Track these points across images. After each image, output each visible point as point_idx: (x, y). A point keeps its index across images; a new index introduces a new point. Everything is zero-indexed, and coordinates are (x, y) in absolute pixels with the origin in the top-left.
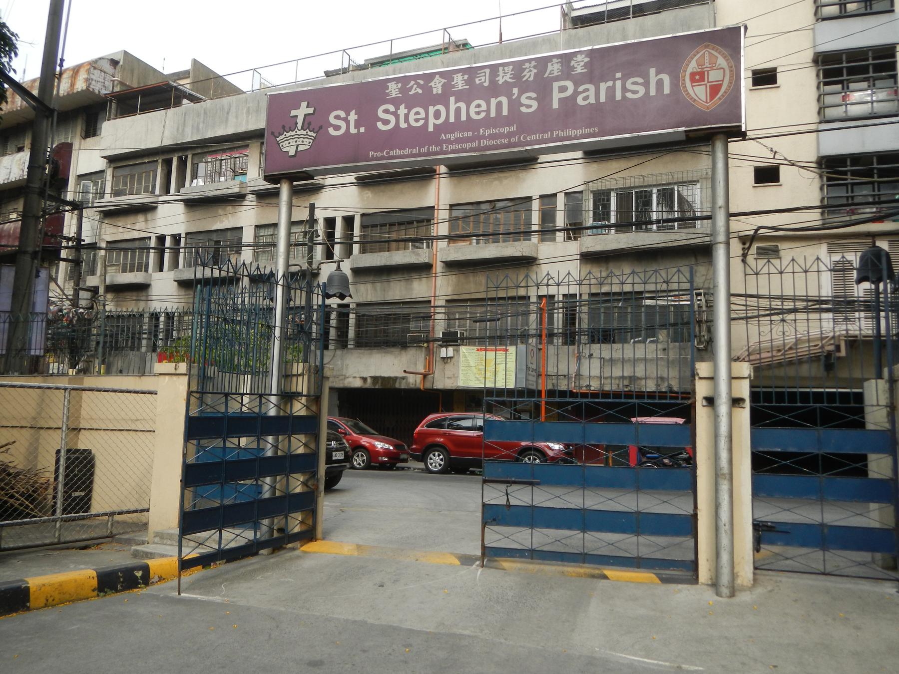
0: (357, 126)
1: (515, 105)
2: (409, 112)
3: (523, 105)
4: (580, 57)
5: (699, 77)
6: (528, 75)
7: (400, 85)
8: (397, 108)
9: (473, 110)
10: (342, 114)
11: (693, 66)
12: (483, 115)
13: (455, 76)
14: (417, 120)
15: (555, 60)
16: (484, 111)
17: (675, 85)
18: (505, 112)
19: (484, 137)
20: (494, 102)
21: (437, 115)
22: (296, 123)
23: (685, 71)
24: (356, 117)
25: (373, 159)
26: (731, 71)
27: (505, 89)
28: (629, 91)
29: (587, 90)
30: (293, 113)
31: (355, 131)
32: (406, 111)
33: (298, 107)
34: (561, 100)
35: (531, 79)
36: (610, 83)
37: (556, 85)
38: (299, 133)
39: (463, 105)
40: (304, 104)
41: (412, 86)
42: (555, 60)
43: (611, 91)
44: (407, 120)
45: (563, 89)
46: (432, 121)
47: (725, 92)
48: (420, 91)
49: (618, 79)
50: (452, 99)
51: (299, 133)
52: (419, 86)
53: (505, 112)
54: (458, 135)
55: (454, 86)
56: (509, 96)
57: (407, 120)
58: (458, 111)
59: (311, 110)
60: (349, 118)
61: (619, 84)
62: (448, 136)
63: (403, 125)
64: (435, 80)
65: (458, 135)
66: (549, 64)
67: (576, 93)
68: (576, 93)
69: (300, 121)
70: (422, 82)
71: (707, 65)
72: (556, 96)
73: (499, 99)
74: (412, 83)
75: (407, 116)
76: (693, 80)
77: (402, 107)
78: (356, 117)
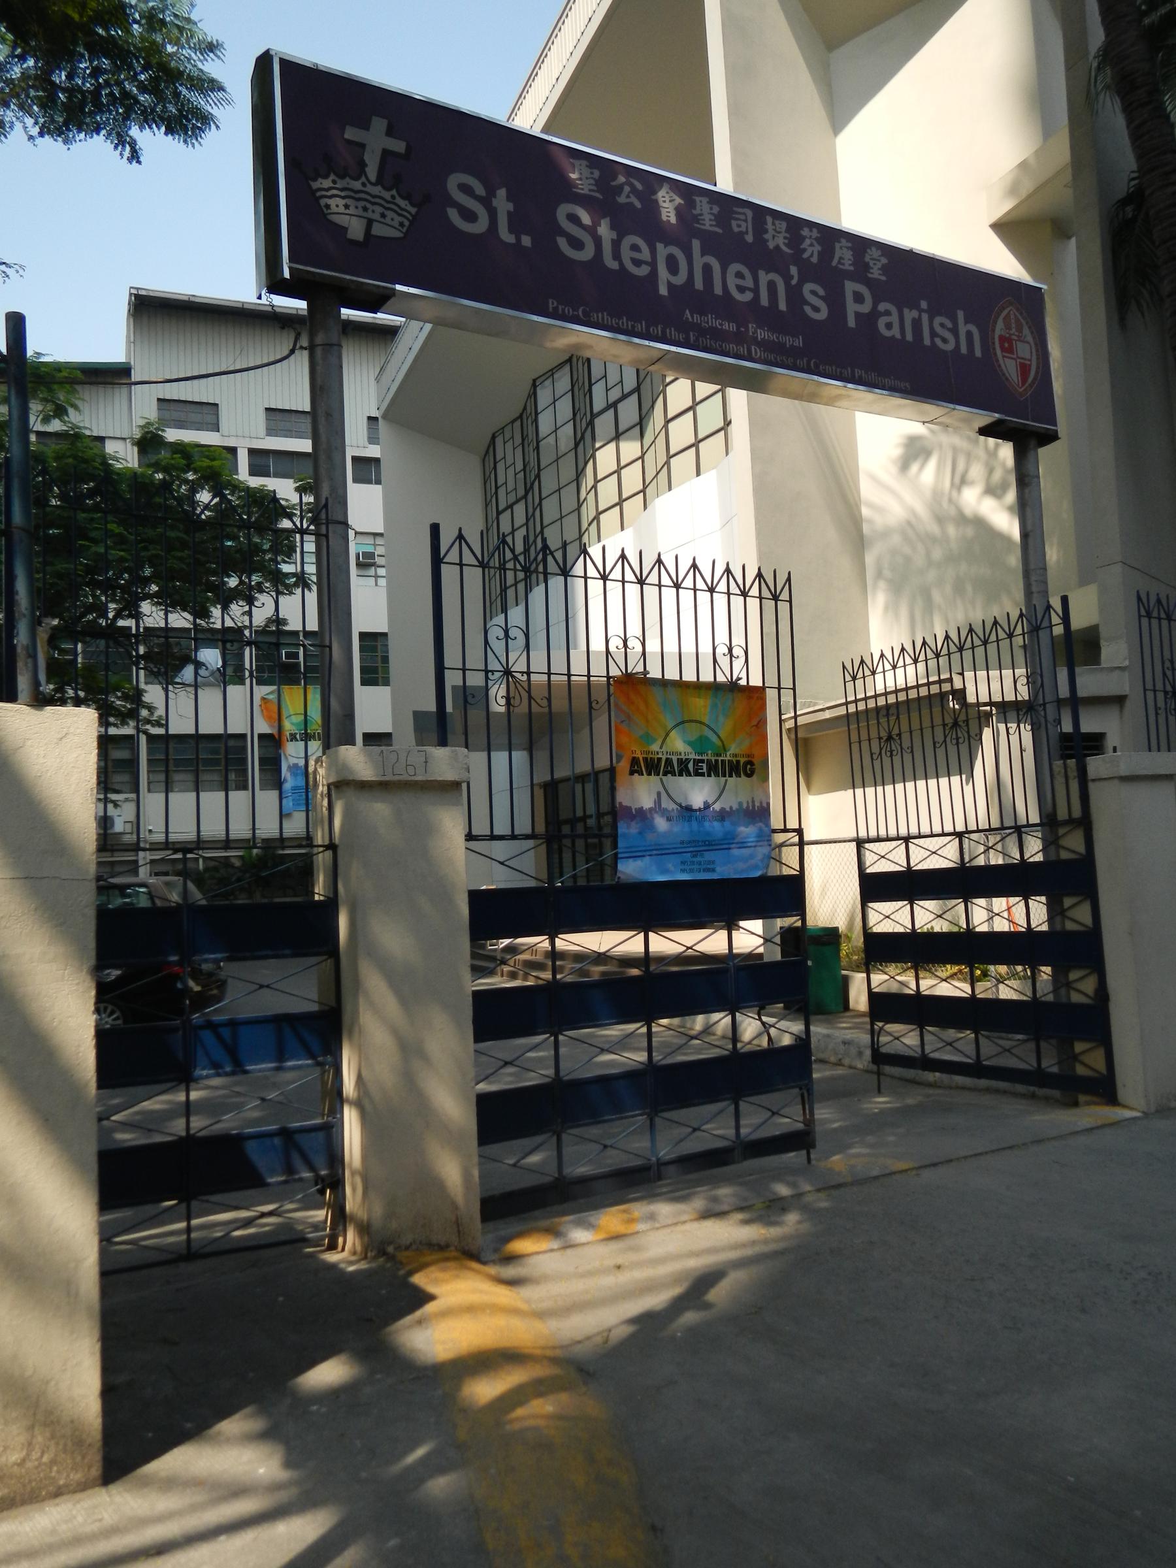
1: (795, 296)
2: (621, 236)
6: (810, 250)
12: (748, 297)
13: (698, 199)
14: (637, 263)
15: (844, 242)
20: (764, 277)
22: (362, 165)
24: (510, 207)
29: (887, 313)
34: (858, 315)
36: (915, 314)
37: (850, 287)
38: (369, 188)
40: (379, 124)
41: (621, 187)
42: (844, 242)
43: (917, 324)
44: (617, 256)
46: (663, 273)
48: (638, 205)
50: (696, 244)
51: (369, 188)
52: (634, 190)
53: (782, 306)
56: (787, 278)
57: (617, 256)
58: (707, 270)
59: (399, 146)
60: (495, 202)
61: (925, 317)
67: (874, 315)
68: (874, 315)
70: (639, 186)
72: (852, 308)
75: (616, 244)
76: (1002, 347)
78: (510, 207)
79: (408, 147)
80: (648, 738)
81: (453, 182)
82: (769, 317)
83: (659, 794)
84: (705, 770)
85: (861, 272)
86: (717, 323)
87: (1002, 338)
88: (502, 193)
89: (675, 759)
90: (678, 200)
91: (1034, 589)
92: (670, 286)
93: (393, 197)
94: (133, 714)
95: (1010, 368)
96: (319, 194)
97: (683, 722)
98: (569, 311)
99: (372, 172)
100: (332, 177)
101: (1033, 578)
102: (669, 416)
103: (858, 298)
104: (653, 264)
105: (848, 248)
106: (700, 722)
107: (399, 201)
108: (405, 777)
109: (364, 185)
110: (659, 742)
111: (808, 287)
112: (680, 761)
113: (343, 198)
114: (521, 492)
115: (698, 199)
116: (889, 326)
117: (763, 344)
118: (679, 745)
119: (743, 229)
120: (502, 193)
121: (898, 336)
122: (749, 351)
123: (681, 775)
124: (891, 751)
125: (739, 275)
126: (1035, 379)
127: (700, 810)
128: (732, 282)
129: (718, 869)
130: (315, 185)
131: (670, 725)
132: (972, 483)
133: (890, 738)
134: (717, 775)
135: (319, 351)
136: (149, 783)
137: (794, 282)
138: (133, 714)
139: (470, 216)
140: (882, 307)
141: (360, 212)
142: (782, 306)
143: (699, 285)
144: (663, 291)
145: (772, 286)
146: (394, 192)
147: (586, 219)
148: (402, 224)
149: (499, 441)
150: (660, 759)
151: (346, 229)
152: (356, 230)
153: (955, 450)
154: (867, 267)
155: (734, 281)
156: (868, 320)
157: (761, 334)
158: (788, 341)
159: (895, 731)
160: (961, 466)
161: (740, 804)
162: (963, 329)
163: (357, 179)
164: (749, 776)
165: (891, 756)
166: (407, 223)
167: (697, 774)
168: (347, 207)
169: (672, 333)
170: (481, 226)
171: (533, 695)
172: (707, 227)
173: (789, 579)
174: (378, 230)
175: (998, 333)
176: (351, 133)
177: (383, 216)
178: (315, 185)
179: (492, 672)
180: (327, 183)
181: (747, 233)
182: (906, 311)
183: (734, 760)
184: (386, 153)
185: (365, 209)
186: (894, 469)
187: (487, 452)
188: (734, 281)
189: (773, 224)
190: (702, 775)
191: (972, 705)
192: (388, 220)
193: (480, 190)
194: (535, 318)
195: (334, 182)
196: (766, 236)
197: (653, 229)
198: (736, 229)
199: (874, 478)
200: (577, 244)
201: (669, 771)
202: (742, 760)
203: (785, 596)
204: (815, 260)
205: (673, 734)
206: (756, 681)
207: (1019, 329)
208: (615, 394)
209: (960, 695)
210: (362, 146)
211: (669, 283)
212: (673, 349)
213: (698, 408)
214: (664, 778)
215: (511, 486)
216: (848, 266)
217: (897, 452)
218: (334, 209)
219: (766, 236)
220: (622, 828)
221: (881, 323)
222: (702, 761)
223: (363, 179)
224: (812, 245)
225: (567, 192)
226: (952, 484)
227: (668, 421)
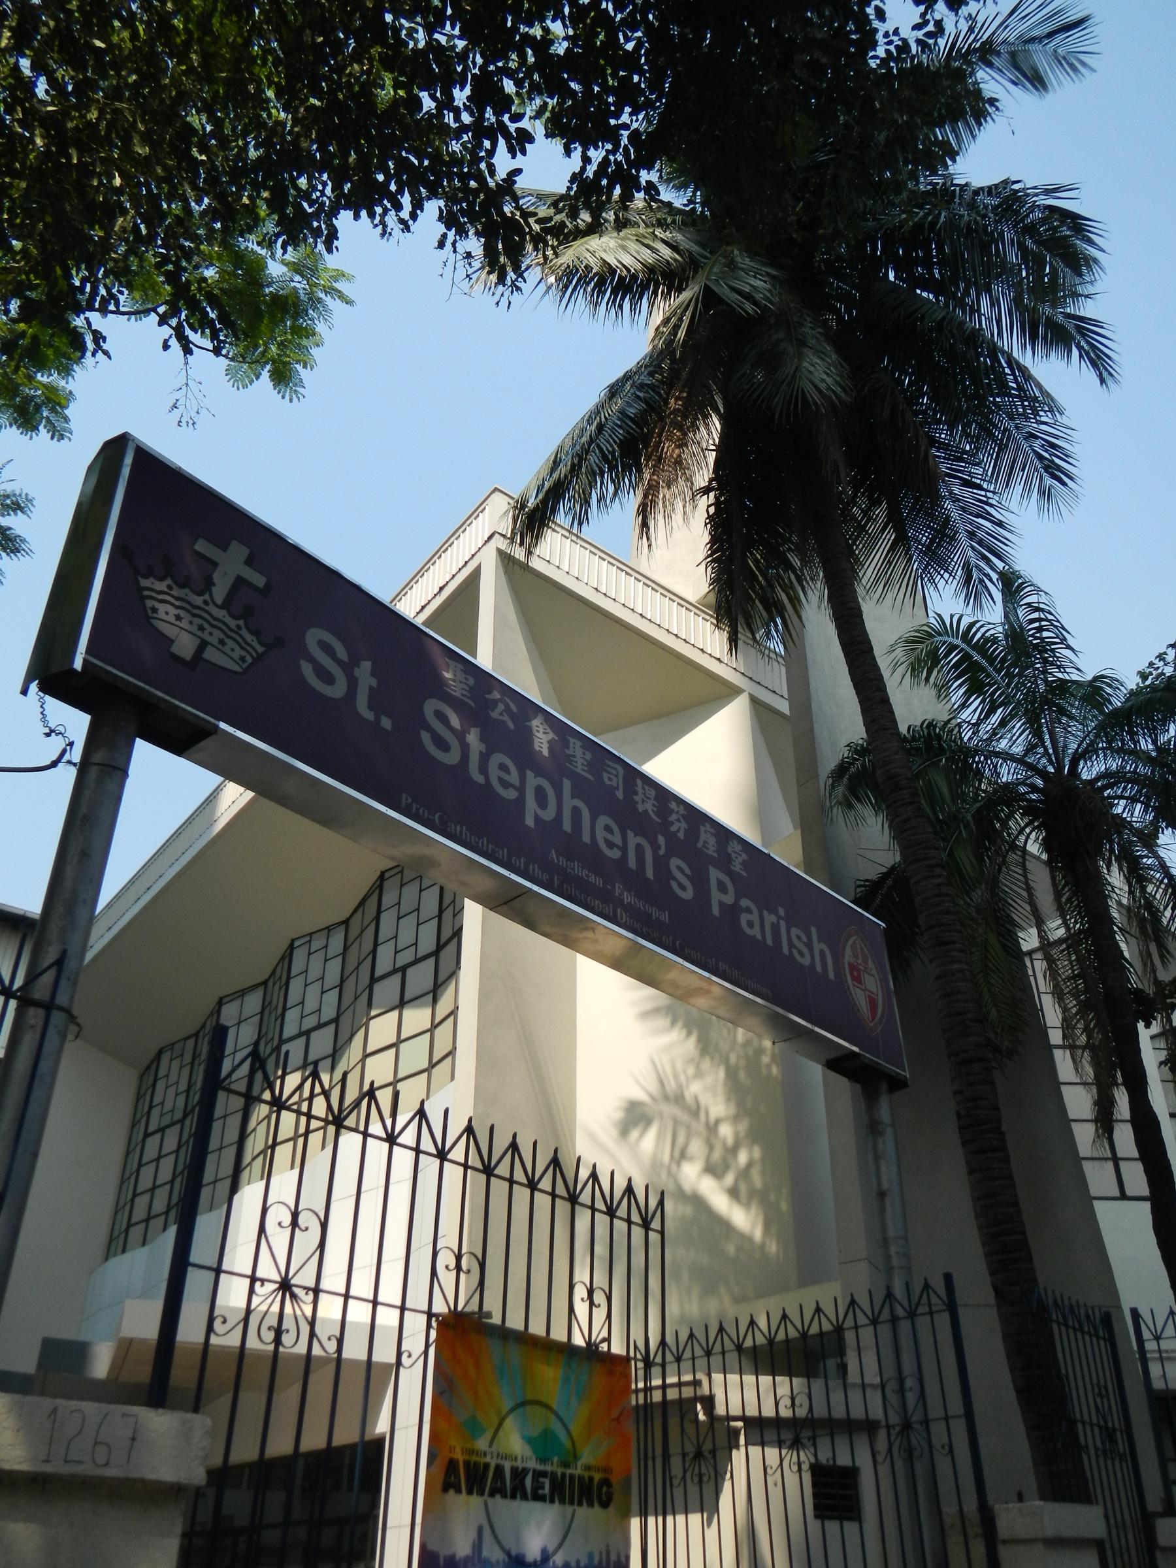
1: (661, 865)
11: (848, 956)
12: (615, 854)
13: (571, 740)
20: (633, 840)
22: (209, 584)
24: (374, 682)
31: (369, 715)
32: (483, 748)
36: (773, 918)
37: (714, 874)
40: (238, 552)
42: (708, 827)
44: (483, 769)
46: (531, 804)
48: (511, 726)
50: (567, 785)
53: (650, 874)
56: (655, 847)
57: (483, 769)
59: (259, 580)
60: (357, 672)
61: (783, 924)
70: (514, 709)
72: (716, 896)
75: (484, 758)
76: (853, 978)
79: (268, 585)
81: (314, 636)
82: (635, 880)
83: (480, 1531)
84: (547, 1490)
85: (724, 862)
86: (583, 873)
87: (850, 964)
88: (367, 665)
89: (507, 1466)
90: (551, 735)
91: (895, 1262)
92: (537, 819)
93: (239, 627)
95: (860, 999)
96: (146, 593)
97: (524, 1404)
99: (219, 593)
100: (169, 582)
101: (893, 1250)
102: (369, 1050)
103: (722, 888)
104: (521, 790)
106: (547, 1407)
107: (244, 632)
108: (87, 1469)
110: (489, 1435)
112: (514, 1470)
113: (177, 607)
114: (179, 1115)
115: (571, 740)
117: (628, 909)
119: (614, 783)
120: (367, 665)
121: (759, 937)
123: (513, 1497)
124: (700, 1476)
125: (607, 828)
126: (882, 1016)
128: (601, 835)
130: (144, 583)
131: (506, 1404)
132: (691, 1159)
133: (699, 1455)
134: (562, 1501)
135: (93, 772)
137: (662, 852)
139: (328, 679)
140: (744, 903)
141: (194, 629)
142: (650, 874)
143: (567, 826)
144: (530, 822)
145: (639, 849)
146: (241, 622)
147: (455, 722)
148: (243, 659)
149: (165, 1058)
150: (487, 1466)
151: (172, 641)
152: (185, 645)
153: (676, 1122)
155: (601, 831)
156: (733, 911)
157: (628, 898)
159: (708, 1446)
160: (681, 1139)
161: (591, 1556)
162: (818, 946)
163: (200, 594)
164: (605, 1505)
165: (700, 1482)
166: (249, 660)
167: (538, 1498)
168: (178, 618)
169: (534, 868)
170: (338, 690)
171: (317, 1329)
173: (661, 1203)
174: (210, 654)
176: (201, 546)
177: (222, 642)
178: (144, 583)
179: (263, 1281)
180: (161, 586)
182: (765, 913)
183: (586, 1475)
184: (239, 582)
185: (201, 628)
186: (614, 1132)
187: (149, 1067)
189: (643, 788)
190: (542, 1499)
191: (720, 1418)
192: (226, 649)
193: (342, 653)
195: (170, 587)
197: (525, 757)
199: (593, 1137)
200: (444, 746)
201: (497, 1490)
202: (597, 1477)
203: (656, 1224)
204: (681, 835)
205: (509, 1422)
206: (617, 1348)
208: (405, 957)
209: (709, 1402)
210: (215, 565)
213: (402, 1046)
214: (491, 1501)
216: (711, 850)
217: (619, 1115)
221: (744, 918)
222: (543, 1474)
223: (207, 597)
224: (678, 820)
225: (438, 689)
226: (672, 1157)
227: (366, 1056)
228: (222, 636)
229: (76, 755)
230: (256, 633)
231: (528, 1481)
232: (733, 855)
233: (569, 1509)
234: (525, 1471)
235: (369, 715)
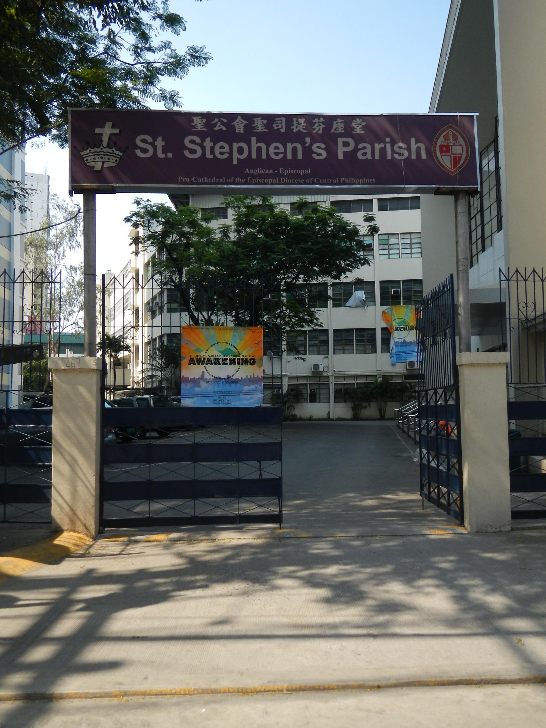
0: (164, 151)
1: (308, 151)
2: (214, 145)
3: (315, 153)
4: (358, 121)
5: (445, 149)
6: (318, 128)
7: (204, 120)
8: (203, 140)
9: (272, 151)
10: (150, 139)
11: (441, 141)
12: (281, 156)
13: (255, 119)
14: (222, 153)
15: (339, 120)
16: (282, 153)
17: (429, 152)
18: (300, 156)
19: (283, 176)
20: (290, 146)
21: (240, 151)
23: (436, 143)
24: (163, 143)
25: (182, 183)
26: (467, 148)
27: (299, 137)
28: (396, 153)
29: (364, 148)
30: (98, 131)
31: (163, 156)
32: (212, 144)
33: (102, 126)
34: (344, 153)
35: (320, 132)
36: (382, 145)
37: (341, 141)
38: (104, 150)
39: (263, 146)
40: (109, 125)
41: (216, 124)
42: (339, 120)
43: (383, 151)
45: (346, 144)
47: (464, 163)
48: (224, 129)
49: (388, 142)
50: (254, 139)
51: (104, 150)
52: (223, 123)
53: (300, 156)
54: (260, 171)
55: (254, 128)
56: (303, 143)
58: (259, 149)
59: (116, 131)
60: (156, 143)
61: (388, 146)
62: (252, 171)
63: (209, 156)
64: (237, 121)
65: (260, 171)
66: (335, 123)
67: (356, 150)
68: (356, 150)
69: (105, 139)
70: (225, 121)
71: (451, 141)
73: (295, 145)
74: (216, 120)
76: (441, 151)
77: (208, 140)
78: (163, 143)
79: (120, 131)
80: (199, 350)
84: (228, 362)
85: (348, 132)
87: (441, 147)
88: (160, 139)
89: (212, 358)
92: (239, 160)
94: (311, 322)
95: (446, 161)
98: (188, 180)
99: (105, 144)
100: (89, 149)
103: (346, 144)
104: (231, 153)
105: (341, 122)
109: (102, 149)
110: (205, 352)
111: (315, 146)
112: (215, 359)
115: (255, 119)
116: (364, 154)
117: (289, 176)
118: (214, 352)
119: (280, 127)
120: (160, 139)
122: (279, 180)
123: (215, 364)
127: (225, 379)
129: (233, 403)
136: (334, 350)
138: (311, 322)
141: (100, 159)
148: (116, 161)
150: (204, 359)
151: (94, 167)
154: (353, 129)
155: (275, 151)
157: (286, 172)
158: (302, 172)
161: (247, 376)
162: (414, 146)
163: (98, 147)
166: (118, 160)
172: (260, 130)
175: (439, 143)
177: (109, 159)
178: (82, 154)
181: (282, 128)
183: (244, 358)
185: (102, 158)
188: (275, 151)
189: (297, 121)
190: (227, 364)
194: (173, 186)
195: (90, 151)
196: (292, 128)
198: (275, 128)
202: (249, 358)
207: (455, 138)
211: (238, 158)
212: (238, 186)
214: (207, 366)
215: (475, 206)
218: (90, 160)
219: (292, 128)
220: (183, 386)
222: (227, 359)
223: (102, 147)
224: (319, 125)
228: (108, 157)
229: (82, 210)
230: (119, 149)
231: (221, 361)
232: (355, 127)
233: (237, 367)
234: (219, 359)
235: (163, 156)
